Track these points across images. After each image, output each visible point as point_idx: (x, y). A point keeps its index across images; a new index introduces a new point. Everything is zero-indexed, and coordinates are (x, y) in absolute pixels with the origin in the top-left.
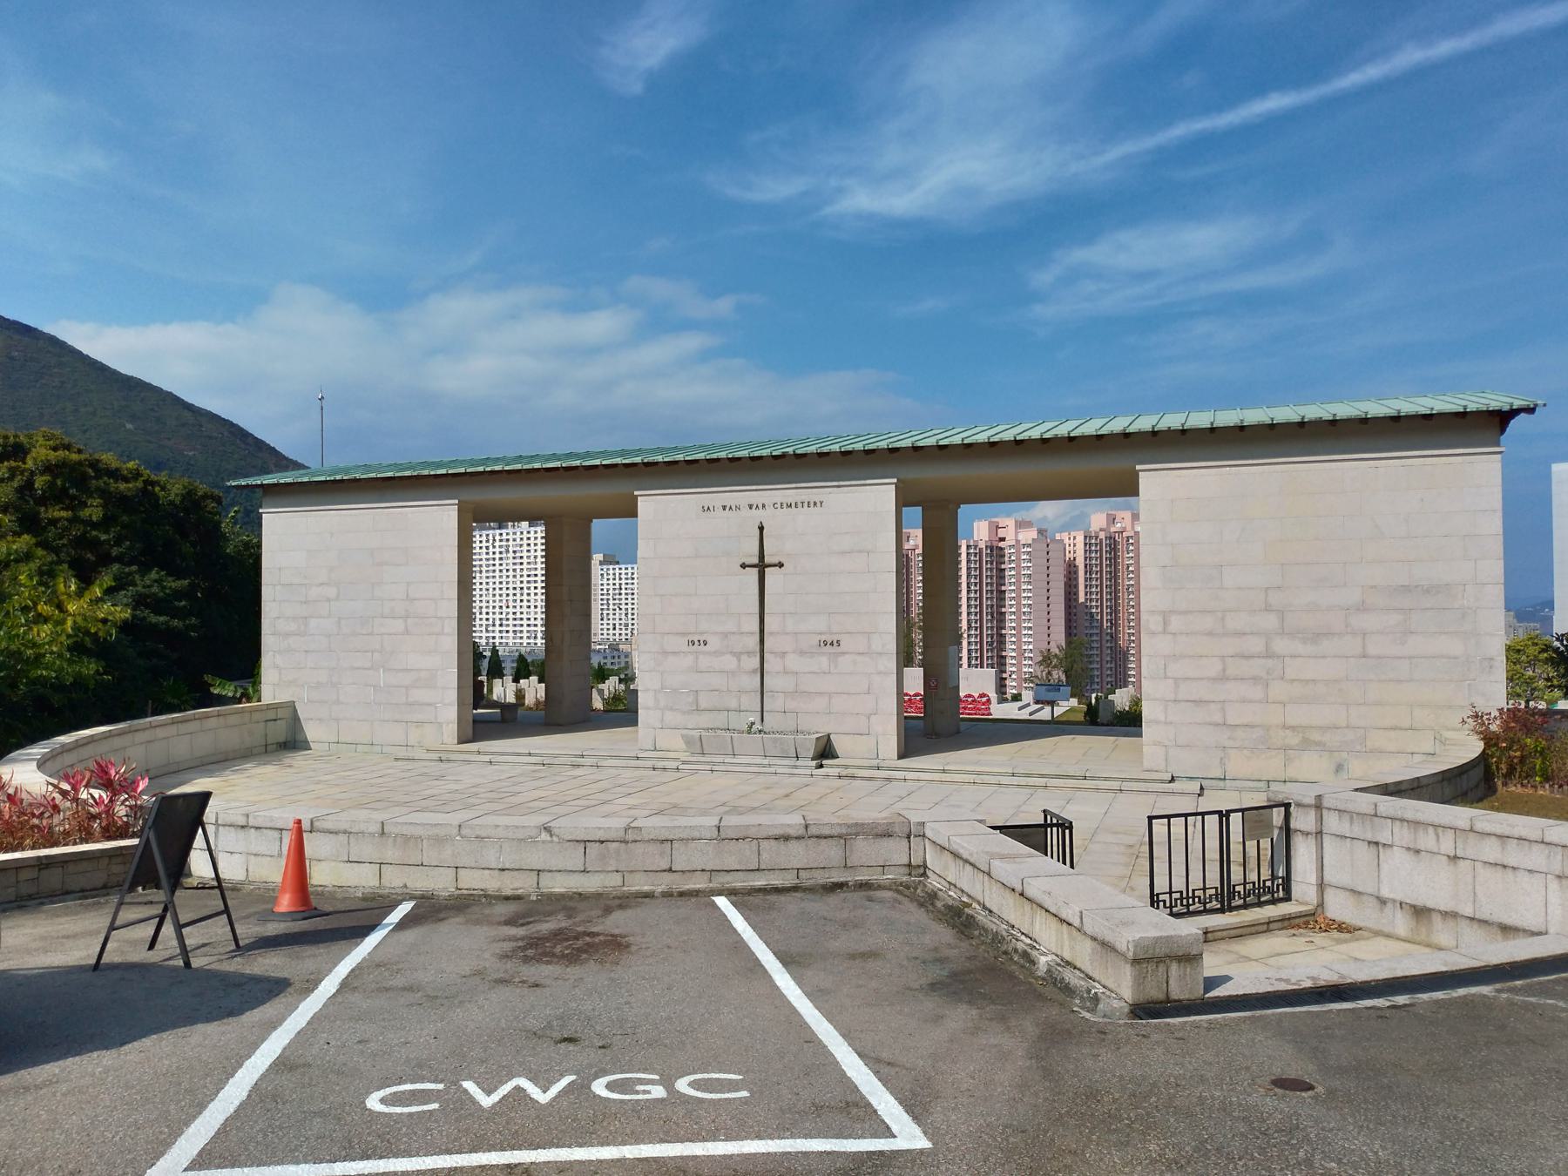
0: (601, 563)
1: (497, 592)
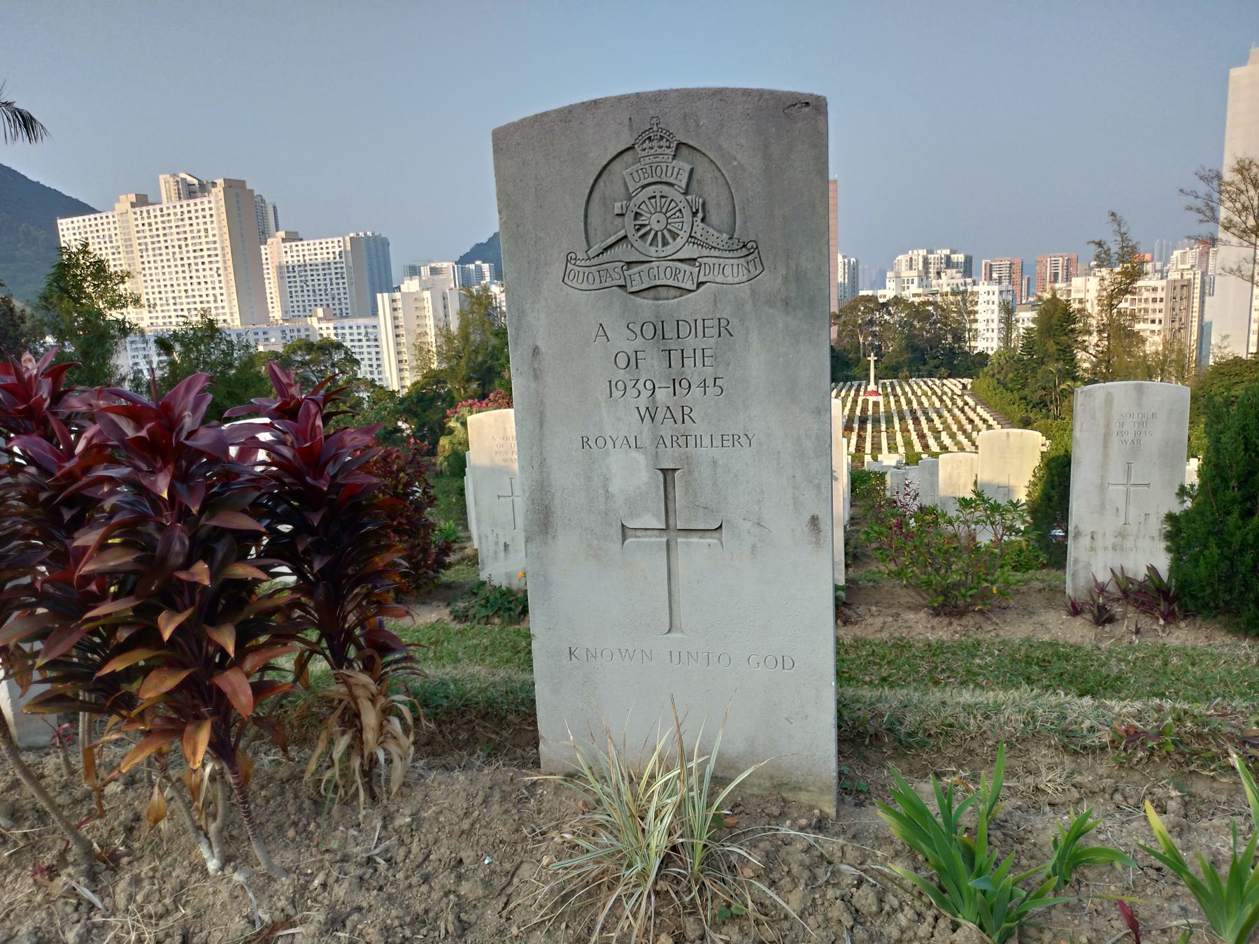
0: (284, 240)
1: (166, 270)
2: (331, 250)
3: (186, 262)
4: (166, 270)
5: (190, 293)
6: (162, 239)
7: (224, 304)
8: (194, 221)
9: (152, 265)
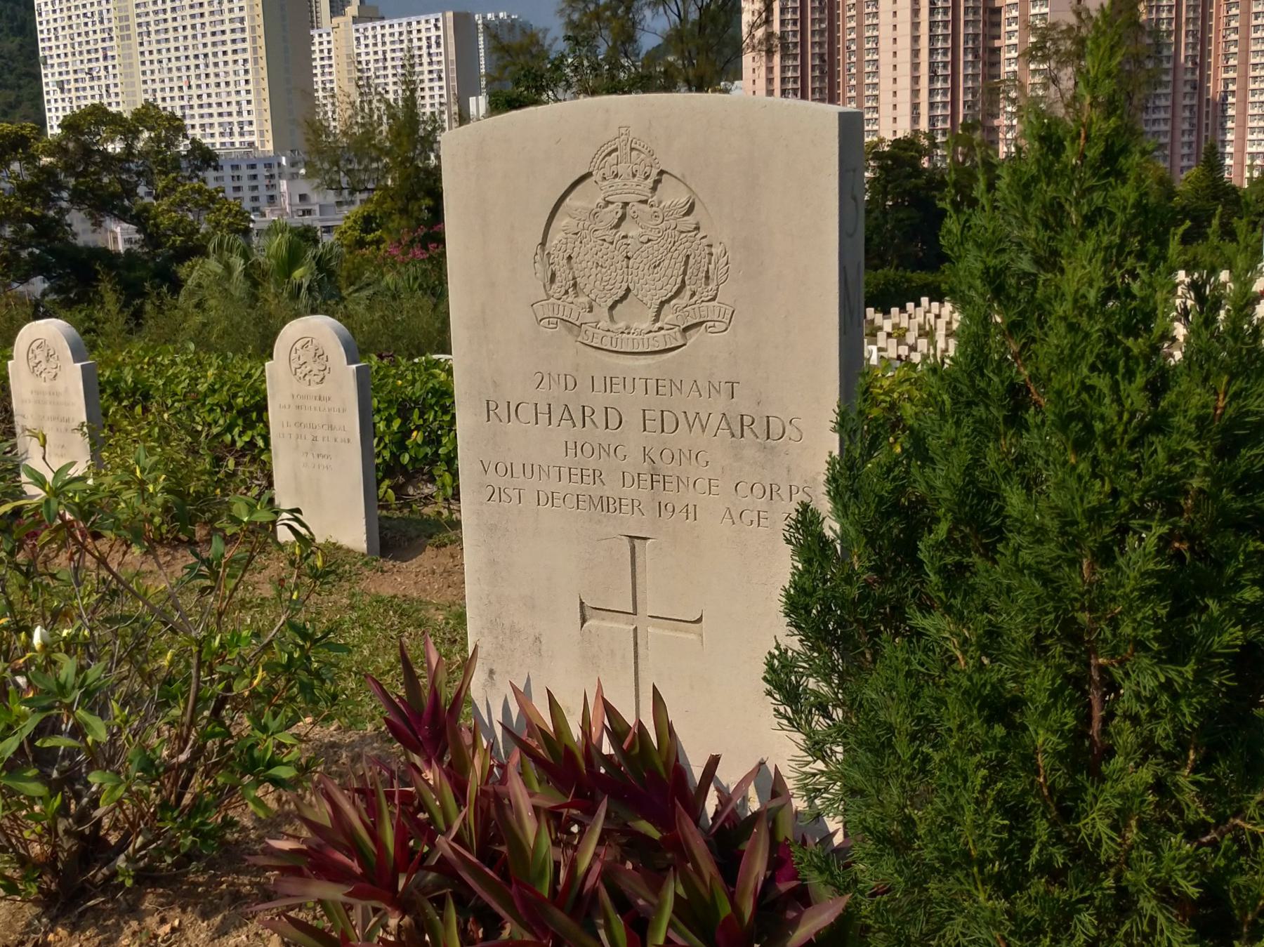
0: (356, 20)
1: (174, 64)
2: (424, 35)
3: (201, 50)
4: (174, 64)
5: (205, 100)
6: (169, 15)
7: (253, 118)
9: (155, 56)
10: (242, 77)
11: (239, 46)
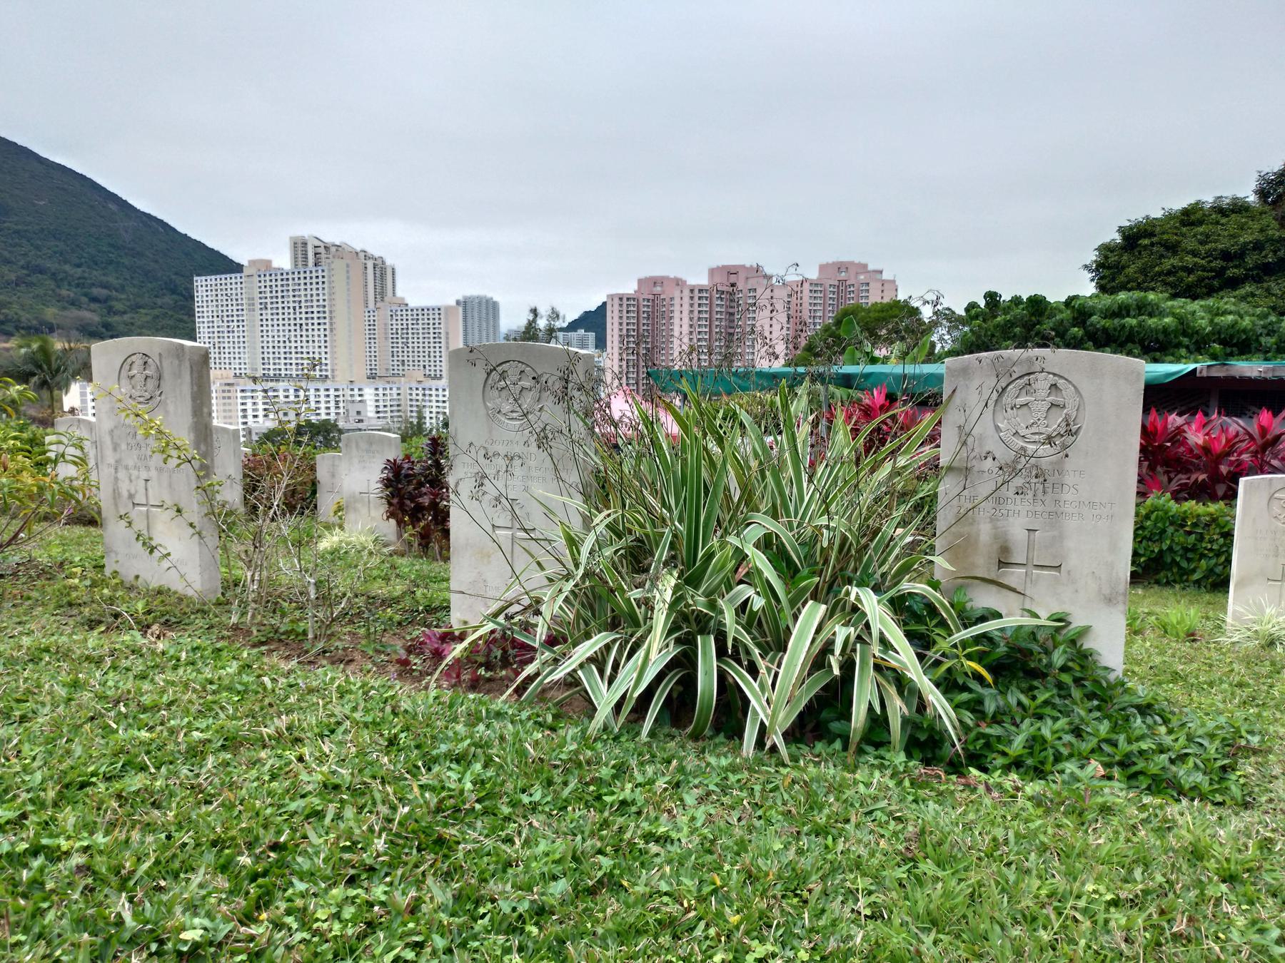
1: (281, 328)
3: (298, 321)
4: (281, 328)
6: (280, 300)
8: (308, 286)
9: (270, 323)
10: (322, 338)
11: (322, 321)
